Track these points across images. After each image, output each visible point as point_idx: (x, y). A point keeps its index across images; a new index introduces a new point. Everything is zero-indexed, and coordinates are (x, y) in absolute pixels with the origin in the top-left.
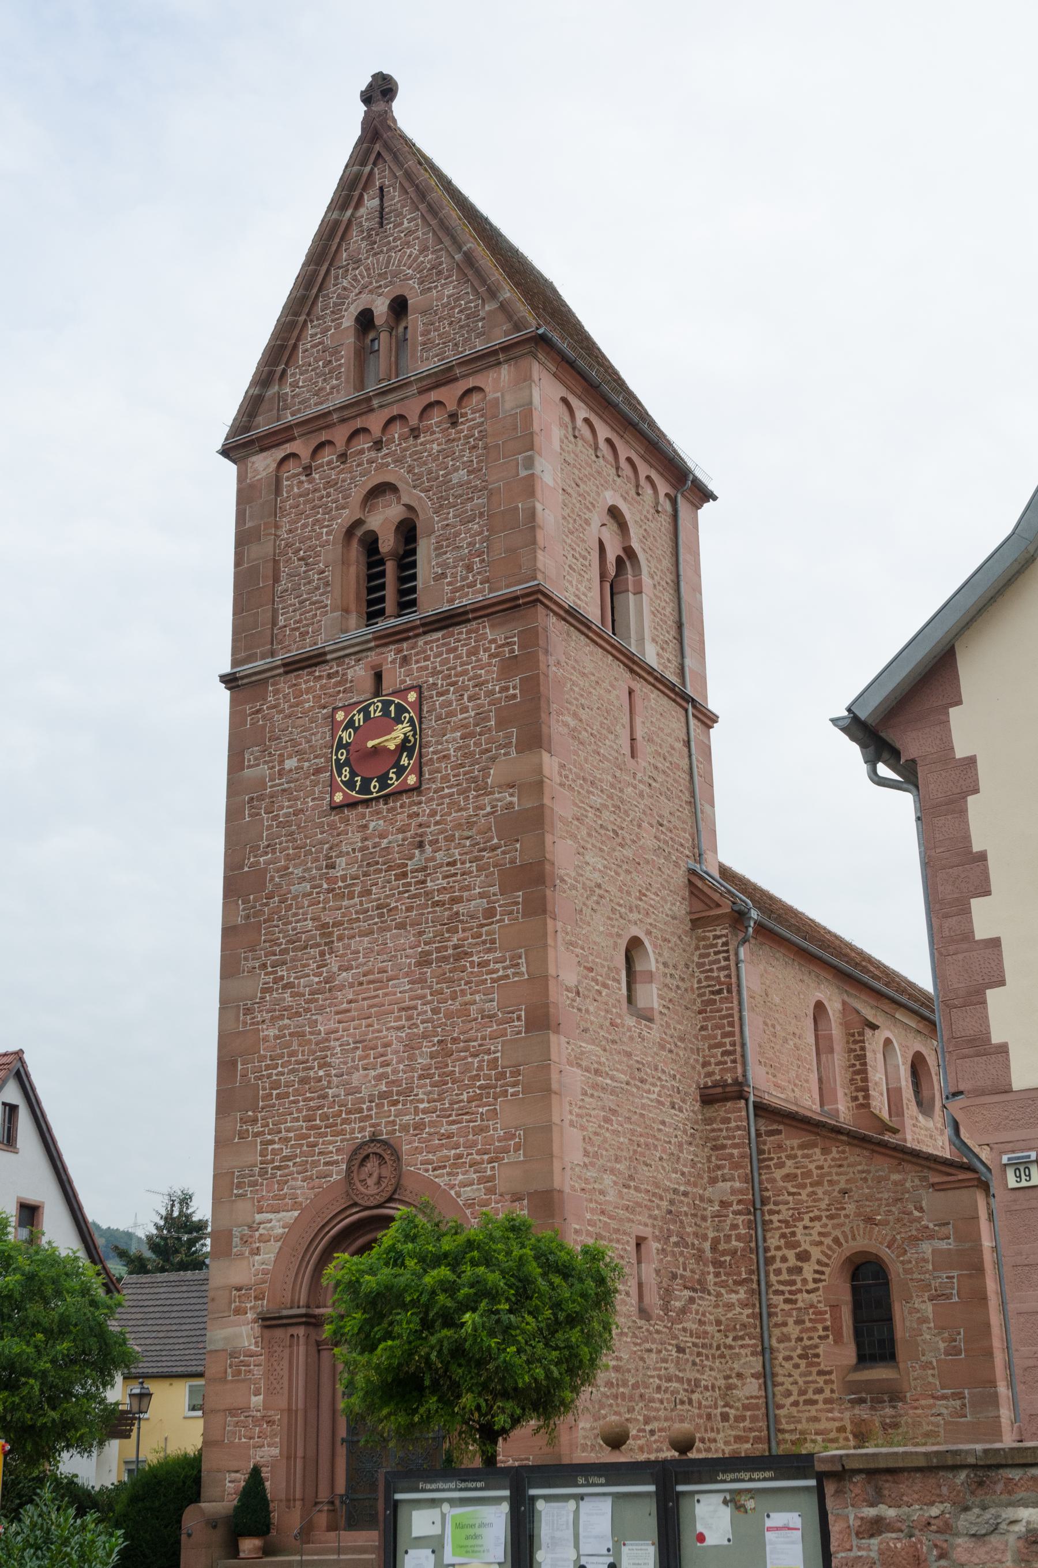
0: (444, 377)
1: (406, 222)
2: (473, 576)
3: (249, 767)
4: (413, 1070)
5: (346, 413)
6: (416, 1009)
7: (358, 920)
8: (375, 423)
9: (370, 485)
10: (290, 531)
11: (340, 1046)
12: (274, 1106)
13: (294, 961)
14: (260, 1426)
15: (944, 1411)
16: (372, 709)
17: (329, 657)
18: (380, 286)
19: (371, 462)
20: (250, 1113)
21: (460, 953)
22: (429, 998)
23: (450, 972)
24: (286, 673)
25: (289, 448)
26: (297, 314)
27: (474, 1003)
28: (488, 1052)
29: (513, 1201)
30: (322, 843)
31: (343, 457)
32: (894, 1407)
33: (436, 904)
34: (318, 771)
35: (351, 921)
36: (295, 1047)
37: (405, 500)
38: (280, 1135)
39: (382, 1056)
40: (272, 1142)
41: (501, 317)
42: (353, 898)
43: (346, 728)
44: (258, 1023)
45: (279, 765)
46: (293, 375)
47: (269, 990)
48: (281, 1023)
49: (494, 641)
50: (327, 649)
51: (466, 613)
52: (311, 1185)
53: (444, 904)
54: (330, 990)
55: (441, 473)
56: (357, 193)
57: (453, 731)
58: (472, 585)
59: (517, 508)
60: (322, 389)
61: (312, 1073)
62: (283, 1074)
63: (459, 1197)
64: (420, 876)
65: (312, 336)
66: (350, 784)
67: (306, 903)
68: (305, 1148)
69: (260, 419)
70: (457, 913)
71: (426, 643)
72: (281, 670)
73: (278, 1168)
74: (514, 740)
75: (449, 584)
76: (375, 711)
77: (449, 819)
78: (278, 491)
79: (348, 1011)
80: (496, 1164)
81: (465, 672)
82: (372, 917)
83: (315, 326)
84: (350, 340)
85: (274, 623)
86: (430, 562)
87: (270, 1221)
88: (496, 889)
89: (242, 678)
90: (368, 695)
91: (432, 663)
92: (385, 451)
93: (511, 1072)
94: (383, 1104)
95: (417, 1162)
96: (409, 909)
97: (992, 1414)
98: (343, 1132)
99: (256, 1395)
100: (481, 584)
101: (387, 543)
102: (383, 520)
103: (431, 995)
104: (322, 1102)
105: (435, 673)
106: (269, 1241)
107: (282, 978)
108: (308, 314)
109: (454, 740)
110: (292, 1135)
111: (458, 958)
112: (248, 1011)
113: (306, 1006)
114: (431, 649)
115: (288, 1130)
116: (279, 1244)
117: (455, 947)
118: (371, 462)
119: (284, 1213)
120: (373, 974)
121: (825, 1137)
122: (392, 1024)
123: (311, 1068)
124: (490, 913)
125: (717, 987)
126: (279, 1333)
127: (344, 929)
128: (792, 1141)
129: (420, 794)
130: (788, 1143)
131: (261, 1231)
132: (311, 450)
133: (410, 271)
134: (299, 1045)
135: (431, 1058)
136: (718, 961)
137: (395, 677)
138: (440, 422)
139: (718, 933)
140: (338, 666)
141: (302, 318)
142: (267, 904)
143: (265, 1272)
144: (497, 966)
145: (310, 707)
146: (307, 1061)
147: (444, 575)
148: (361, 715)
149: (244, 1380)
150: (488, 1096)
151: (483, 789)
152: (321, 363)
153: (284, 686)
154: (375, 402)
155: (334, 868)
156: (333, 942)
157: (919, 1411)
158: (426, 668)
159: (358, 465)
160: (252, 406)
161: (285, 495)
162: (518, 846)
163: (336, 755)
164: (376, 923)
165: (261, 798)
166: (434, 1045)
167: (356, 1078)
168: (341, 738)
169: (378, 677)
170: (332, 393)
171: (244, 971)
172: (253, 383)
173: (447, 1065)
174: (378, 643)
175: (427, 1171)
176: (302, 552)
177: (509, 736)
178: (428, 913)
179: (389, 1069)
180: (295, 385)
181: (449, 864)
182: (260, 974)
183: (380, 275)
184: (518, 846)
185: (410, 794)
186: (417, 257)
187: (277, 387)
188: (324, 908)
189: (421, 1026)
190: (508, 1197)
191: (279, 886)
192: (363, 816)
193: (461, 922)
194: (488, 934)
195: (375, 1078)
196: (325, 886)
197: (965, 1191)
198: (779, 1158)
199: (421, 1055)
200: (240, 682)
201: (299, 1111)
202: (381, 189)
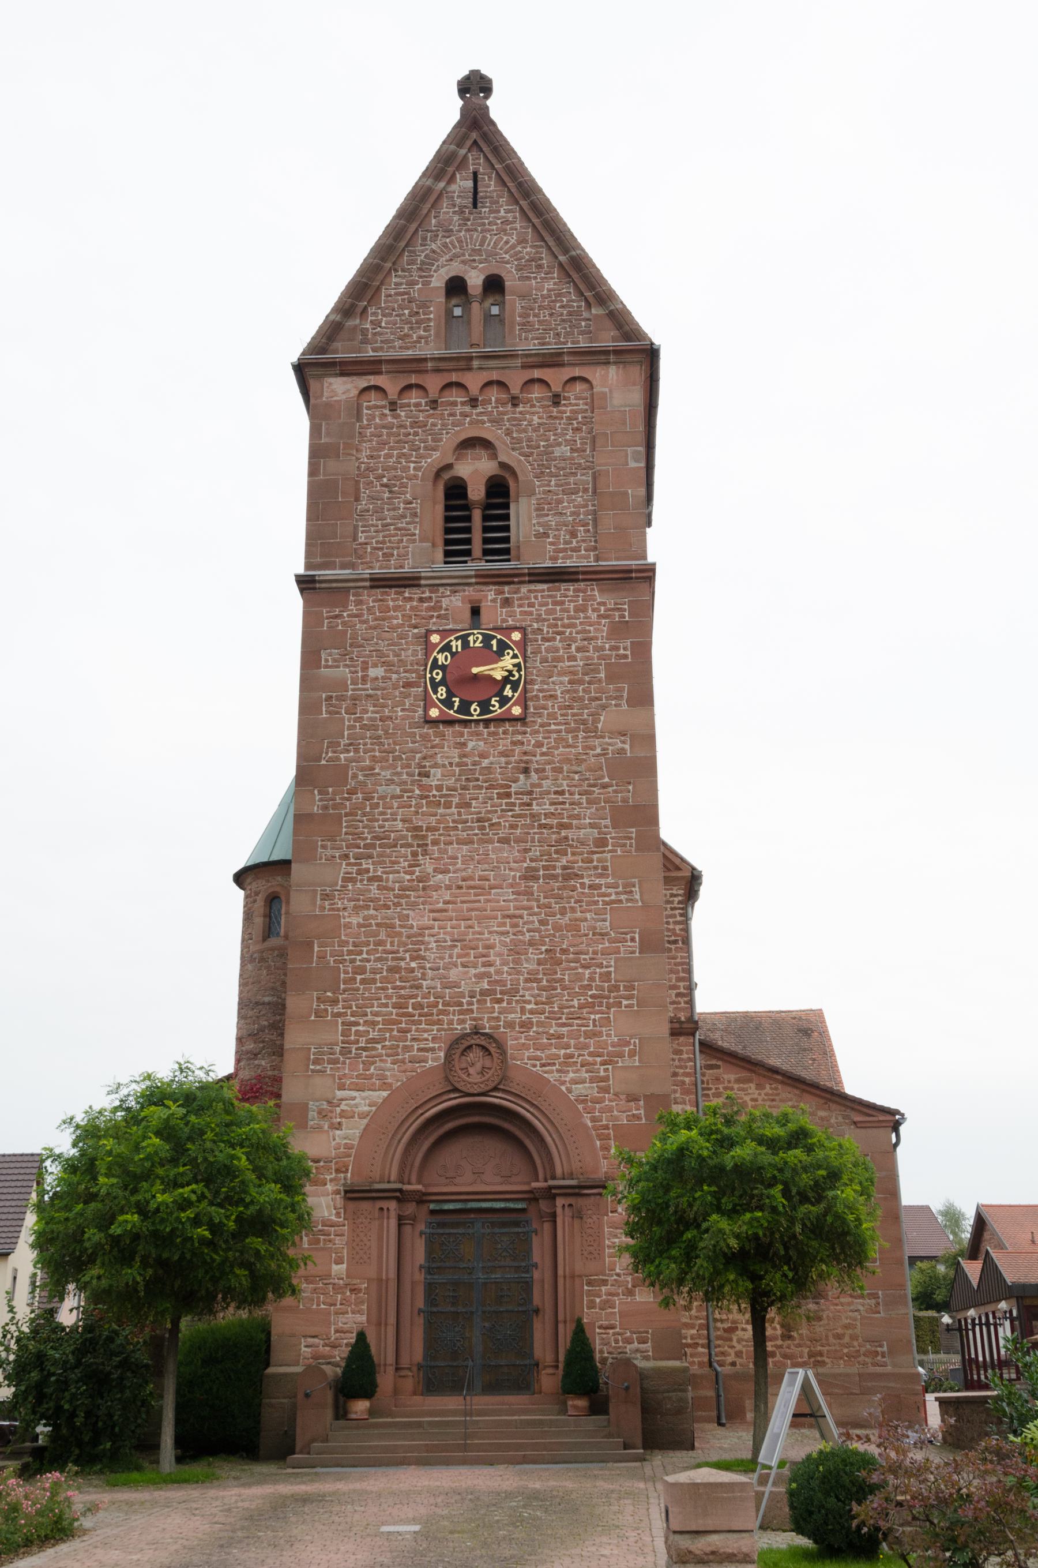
0: (553, 360)
1: (502, 211)
2: (577, 542)
3: (326, 667)
4: (519, 973)
6: (522, 918)
7: (456, 828)
8: (474, 381)
9: (464, 436)
11: (436, 942)
12: (358, 989)
13: (382, 856)
14: (343, 1293)
15: (861, 1308)
16: (471, 638)
17: (423, 582)
18: (474, 260)
19: (464, 415)
20: (329, 994)
21: (569, 875)
22: (536, 910)
23: (559, 889)
24: (372, 587)
26: (384, 259)
27: (586, 920)
28: (601, 966)
29: (629, 1101)
30: (414, 751)
31: (434, 404)
32: (817, 1303)
33: (541, 826)
34: (408, 685)
36: (382, 936)
37: (503, 458)
38: (365, 1018)
39: (484, 956)
40: (357, 1024)
41: (608, 323)
42: (450, 807)
43: (442, 651)
44: (338, 910)
45: (362, 671)
46: (374, 314)
47: (353, 880)
48: (366, 913)
49: (604, 604)
50: (423, 574)
51: (577, 573)
52: (402, 1069)
53: (552, 828)
54: (424, 889)
55: (542, 443)
56: (451, 169)
57: (559, 674)
58: (577, 550)
59: (627, 493)
60: (407, 336)
61: (403, 964)
62: (368, 961)
63: (570, 1092)
64: (526, 799)
65: (396, 284)
66: (448, 703)
67: (396, 805)
68: (395, 1033)
69: (338, 345)
70: (566, 838)
72: (367, 584)
73: (364, 1049)
74: (625, 695)
75: (551, 544)
76: (475, 642)
77: (556, 752)
78: (359, 417)
79: (446, 911)
80: (610, 1067)
81: (574, 626)
82: (472, 828)
83: (400, 276)
84: (442, 299)
85: (355, 539)
86: (530, 520)
87: (354, 1098)
88: (608, 822)
89: (321, 582)
90: (467, 626)
91: (537, 610)
92: (480, 409)
93: (625, 986)
94: (486, 1001)
95: (524, 1056)
96: (513, 827)
97: (903, 1312)
99: (337, 1264)
100: (586, 550)
101: (476, 492)
102: (475, 471)
103: (538, 907)
104: (415, 991)
106: (353, 1117)
107: (367, 871)
109: (561, 683)
110: (380, 1019)
111: (567, 878)
112: (326, 897)
113: (396, 900)
114: (536, 598)
115: (376, 1014)
116: (365, 1121)
117: (564, 868)
118: (464, 415)
119: (371, 1093)
120: (473, 879)
121: (759, 1075)
122: (495, 929)
124: (601, 842)
125: (673, 938)
126: (365, 1205)
127: (440, 835)
128: (729, 1075)
130: (726, 1076)
131: (343, 1107)
132: (399, 388)
133: (507, 256)
134: (388, 936)
135: (539, 964)
136: (675, 916)
137: (494, 613)
138: (542, 398)
139: (674, 892)
140: (431, 592)
141: (389, 265)
142: (348, 799)
143: (348, 1147)
144: (609, 890)
145: (398, 624)
146: (397, 952)
147: (546, 535)
148: (459, 642)
149: (323, 1249)
150: (601, 1005)
151: (592, 731)
152: (406, 312)
153: (370, 599)
154: (476, 363)
155: (428, 777)
156: (427, 845)
157: (839, 1307)
158: (531, 613)
160: (331, 331)
161: (365, 422)
162: (631, 787)
164: (476, 835)
165: (341, 698)
166: (541, 953)
168: (436, 660)
169: (476, 612)
170: (420, 342)
171: (321, 859)
172: (336, 309)
173: (556, 973)
174: (478, 580)
175: (535, 1066)
176: (385, 480)
177: (620, 690)
178: (535, 833)
179: (492, 970)
180: (376, 324)
181: (556, 793)
182: (341, 864)
183: (473, 250)
184: (631, 787)
185: (514, 723)
186: (513, 247)
188: (417, 813)
189: (527, 934)
190: (623, 1097)
191: (364, 784)
192: (462, 735)
193: (571, 846)
194: (599, 860)
195: (475, 976)
196: (417, 792)
197: (882, 1130)
198: (716, 1089)
199: (527, 960)
200: (318, 585)
201: (387, 997)
202: (475, 174)
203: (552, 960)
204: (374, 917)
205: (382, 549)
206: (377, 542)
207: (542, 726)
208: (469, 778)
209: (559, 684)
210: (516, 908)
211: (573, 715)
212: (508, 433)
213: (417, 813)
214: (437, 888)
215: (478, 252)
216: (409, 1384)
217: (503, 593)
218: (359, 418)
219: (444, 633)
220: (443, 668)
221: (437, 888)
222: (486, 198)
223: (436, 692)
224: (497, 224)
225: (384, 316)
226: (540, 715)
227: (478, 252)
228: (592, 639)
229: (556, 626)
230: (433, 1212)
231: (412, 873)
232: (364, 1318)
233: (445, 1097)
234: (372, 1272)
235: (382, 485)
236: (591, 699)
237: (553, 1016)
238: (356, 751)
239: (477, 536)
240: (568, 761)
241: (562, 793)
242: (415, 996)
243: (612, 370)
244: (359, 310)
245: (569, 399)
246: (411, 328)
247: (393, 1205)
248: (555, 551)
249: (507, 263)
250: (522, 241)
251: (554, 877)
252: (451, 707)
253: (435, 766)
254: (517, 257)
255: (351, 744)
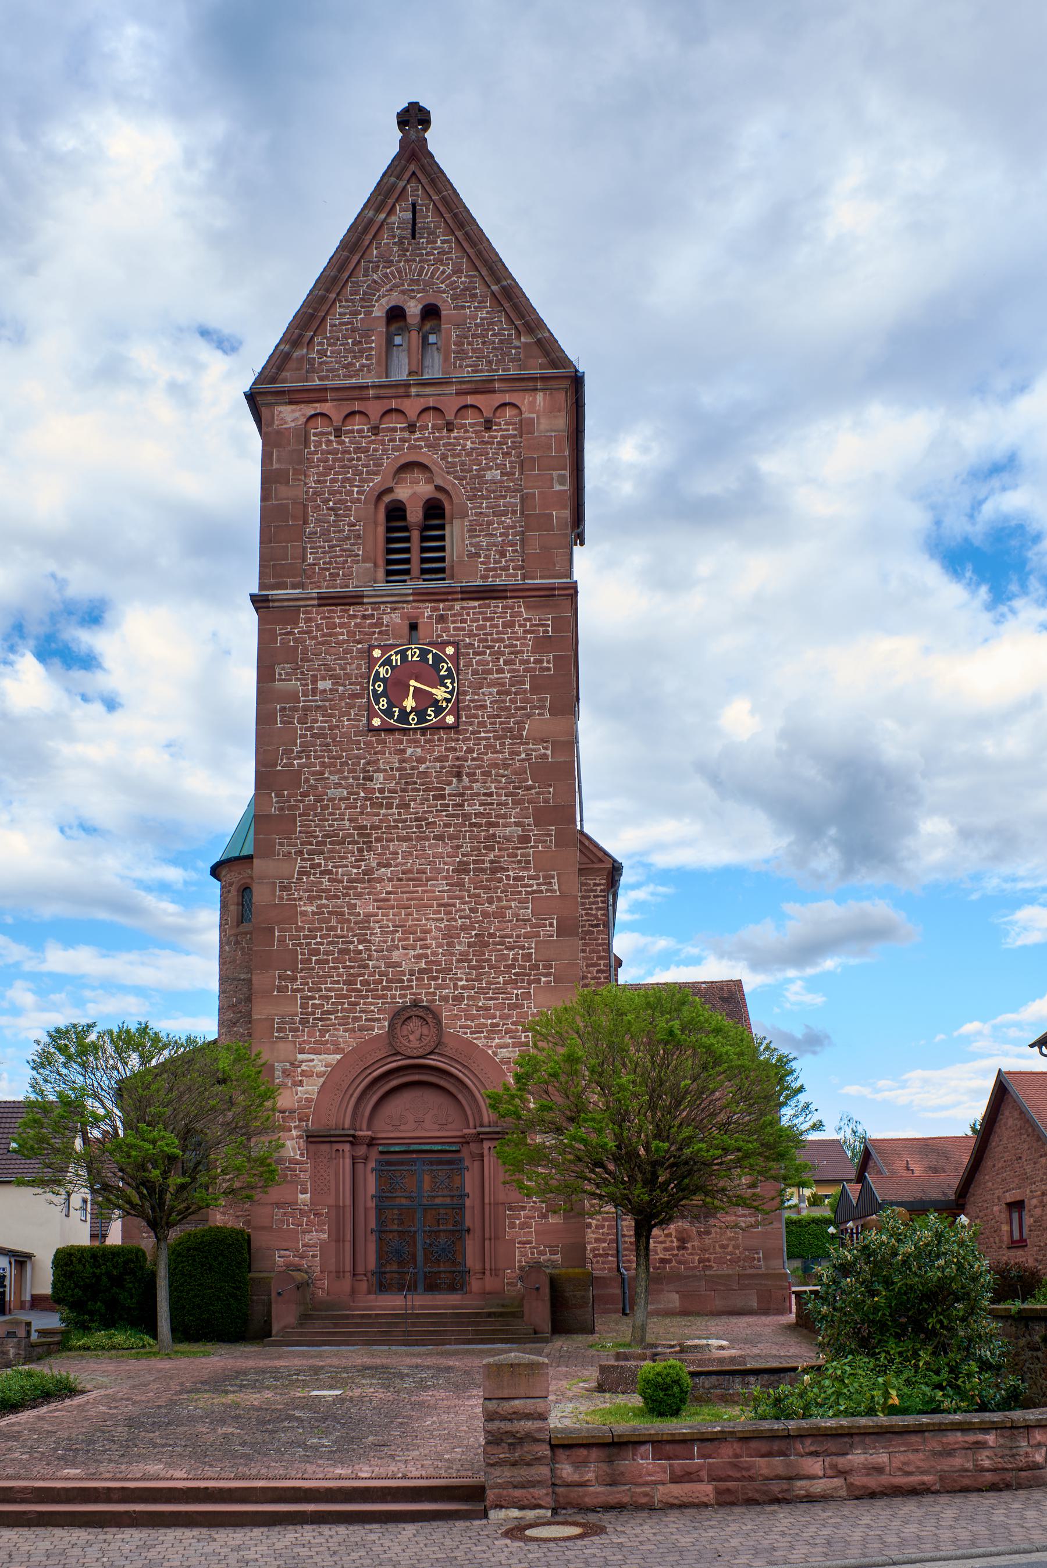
0: (484, 388)
2: (506, 562)
3: (281, 680)
4: (452, 954)
5: (383, 392)
7: (397, 827)
8: (412, 407)
9: (403, 461)
10: (318, 482)
12: (313, 969)
14: (308, 1217)
16: (409, 653)
17: (366, 600)
18: (413, 290)
19: (403, 440)
21: (496, 868)
24: (320, 605)
25: (319, 407)
26: (328, 290)
28: (523, 948)
31: (375, 430)
33: (472, 825)
35: (388, 827)
36: (333, 923)
37: (439, 482)
40: (313, 998)
41: (536, 351)
43: (383, 665)
44: (295, 899)
46: (321, 344)
47: (308, 874)
49: (529, 620)
51: (505, 591)
54: (369, 881)
57: (489, 686)
58: (505, 569)
61: (351, 947)
62: (322, 944)
66: (388, 712)
67: (343, 806)
68: (346, 1006)
69: (286, 374)
70: (494, 835)
71: (462, 608)
72: (315, 602)
75: (482, 563)
76: (413, 656)
79: (388, 900)
81: (502, 640)
82: (411, 827)
83: (344, 307)
84: (382, 328)
85: (304, 560)
86: (463, 541)
87: (312, 1060)
90: (405, 641)
92: (417, 435)
95: (458, 1025)
98: (384, 997)
101: (415, 515)
102: (412, 492)
104: (363, 971)
105: (471, 635)
107: (320, 865)
108: (338, 294)
109: (490, 694)
111: (494, 871)
112: (284, 888)
114: (468, 614)
116: (322, 1080)
117: (492, 862)
120: (412, 873)
123: (352, 942)
124: (524, 839)
126: (325, 1148)
129: (457, 732)
131: (304, 1067)
133: (443, 286)
134: (338, 922)
135: (469, 947)
137: (431, 628)
138: (474, 424)
140: (373, 609)
141: (333, 296)
142: (302, 801)
148: (399, 657)
150: (523, 981)
152: (350, 341)
154: (413, 390)
158: (464, 629)
159: (390, 440)
160: (279, 361)
163: (373, 685)
164: (415, 832)
165: (294, 709)
167: (396, 955)
168: (377, 673)
169: (413, 627)
170: (362, 371)
171: (279, 855)
174: (416, 598)
175: (466, 1033)
176: (331, 503)
177: (544, 700)
179: (429, 951)
180: (322, 353)
181: (485, 794)
183: (412, 280)
185: (448, 731)
186: (449, 277)
187: (305, 350)
188: (362, 813)
193: (498, 843)
196: (362, 794)
200: (271, 604)
202: (414, 205)
203: (481, 943)
204: (327, 906)
205: (328, 569)
206: (324, 563)
207: (473, 733)
208: (407, 782)
209: (489, 695)
210: (449, 897)
211: (501, 723)
212: (444, 457)
213: (362, 813)
214: (380, 880)
215: (417, 282)
216: (363, 1286)
217: (439, 610)
218: (307, 444)
219: (385, 649)
220: (384, 680)
221: (380, 880)
222: (424, 228)
223: (378, 703)
224: (434, 254)
225: (329, 345)
226: (471, 724)
227: (417, 282)
228: (518, 652)
229: (486, 640)
230: (382, 1153)
231: (359, 867)
232: (326, 1236)
233: (390, 1059)
234: (331, 1201)
235: (328, 509)
236: (517, 709)
237: (482, 991)
238: (308, 757)
239: (415, 556)
240: (496, 765)
241: (491, 794)
242: (363, 975)
243: (540, 397)
244: (306, 340)
245: (499, 424)
246: (355, 357)
247: (347, 1147)
248: (486, 570)
249: (444, 292)
250: (457, 271)
251: (483, 870)
252: (391, 717)
253: (378, 770)
254: (452, 286)
255: (302, 752)
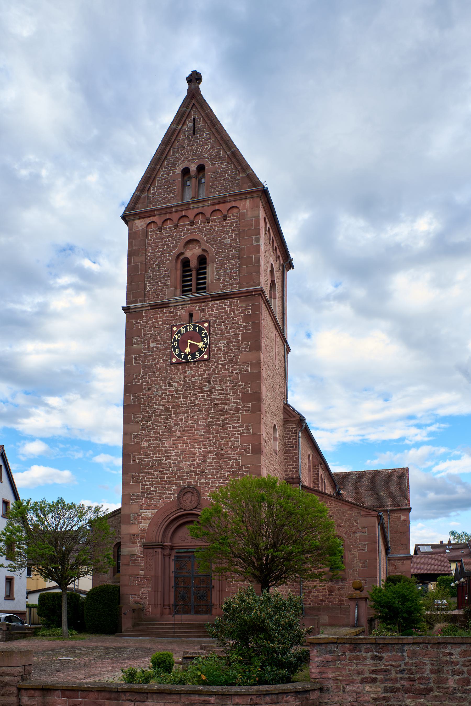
0: (223, 201)
2: (232, 281)
3: (135, 344)
4: (205, 463)
5: (179, 208)
8: (191, 214)
9: (188, 239)
10: (152, 253)
14: (143, 581)
16: (189, 327)
17: (170, 305)
18: (193, 159)
19: (188, 230)
21: (225, 423)
24: (151, 309)
25: (152, 219)
26: (156, 165)
27: (231, 441)
28: (236, 459)
30: (167, 376)
31: (176, 226)
33: (216, 404)
34: (165, 349)
35: (179, 407)
36: (155, 451)
37: (203, 247)
43: (177, 334)
44: (139, 442)
47: (145, 430)
49: (241, 307)
51: (230, 295)
53: (219, 404)
54: (170, 432)
57: (223, 340)
58: (232, 284)
60: (166, 197)
62: (150, 461)
66: (179, 355)
67: (160, 399)
70: (224, 408)
71: (212, 305)
72: (149, 308)
75: (222, 283)
76: (190, 329)
79: (178, 440)
81: (229, 318)
84: (180, 179)
85: (145, 289)
86: (213, 273)
87: (146, 512)
90: (187, 322)
92: (194, 226)
98: (176, 483)
101: (194, 263)
102: (192, 253)
105: (216, 317)
107: (150, 426)
108: (161, 166)
109: (224, 343)
111: (224, 425)
112: (135, 437)
114: (214, 307)
117: (223, 421)
118: (188, 230)
123: (163, 460)
124: (238, 409)
126: (151, 550)
127: (176, 410)
129: (209, 362)
132: (162, 221)
133: (206, 155)
134: (157, 451)
135: (213, 460)
137: (198, 316)
141: (158, 167)
142: (143, 398)
143: (144, 530)
148: (184, 330)
151: (235, 363)
152: (166, 187)
154: (192, 206)
158: (212, 314)
159: (183, 230)
163: (173, 343)
164: (190, 409)
165: (140, 357)
167: (181, 465)
168: (175, 337)
169: (191, 315)
170: (171, 200)
171: (133, 422)
174: (192, 302)
177: (247, 344)
179: (195, 462)
181: (221, 390)
183: (193, 154)
186: (209, 150)
187: (146, 193)
188: (168, 402)
193: (226, 412)
194: (236, 417)
196: (168, 393)
199: (209, 458)
200: (131, 311)
202: (194, 119)
203: (218, 458)
204: (153, 444)
205: (155, 292)
206: (154, 290)
207: (216, 362)
208: (187, 386)
209: (223, 344)
210: (204, 438)
211: (228, 356)
212: (205, 235)
213: (168, 402)
214: (175, 431)
215: (195, 155)
216: (167, 611)
217: (202, 306)
218: (147, 236)
219: (178, 326)
220: (178, 341)
221: (175, 431)
222: (198, 129)
223: (175, 351)
224: (202, 141)
225: (157, 190)
226: (215, 358)
227: (195, 155)
228: (236, 323)
229: (222, 319)
231: (166, 426)
232: (151, 589)
233: (178, 511)
235: (156, 265)
236: (235, 349)
237: (218, 480)
238: (146, 378)
239: (194, 283)
240: (225, 376)
241: (223, 390)
242: (167, 474)
243: (248, 202)
244: (147, 189)
245: (230, 217)
246: (168, 194)
247: (160, 550)
248: (223, 286)
249: (207, 158)
250: (213, 147)
251: (219, 425)
252: (180, 357)
253: (175, 382)
254: (211, 155)
255: (143, 376)
